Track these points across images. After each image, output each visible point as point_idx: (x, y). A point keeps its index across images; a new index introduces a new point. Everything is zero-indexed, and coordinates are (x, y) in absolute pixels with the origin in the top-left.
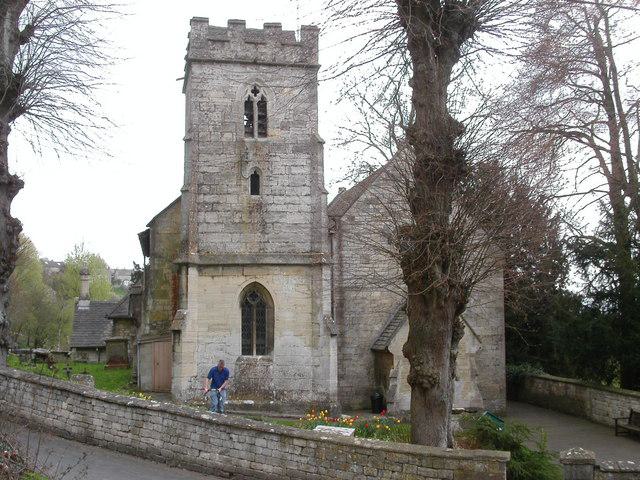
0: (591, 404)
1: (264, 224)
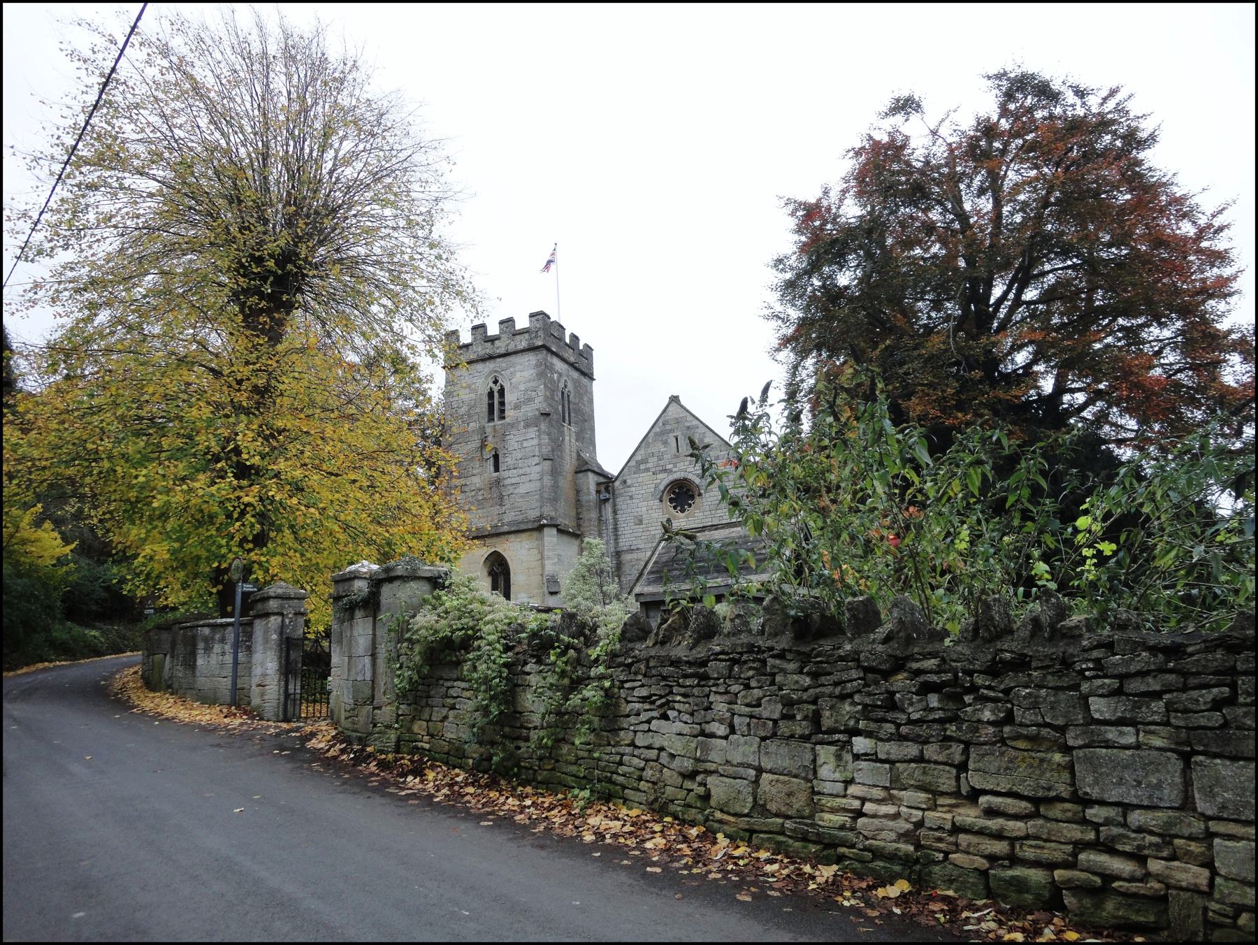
0: (552, 629)
1: (501, 497)
